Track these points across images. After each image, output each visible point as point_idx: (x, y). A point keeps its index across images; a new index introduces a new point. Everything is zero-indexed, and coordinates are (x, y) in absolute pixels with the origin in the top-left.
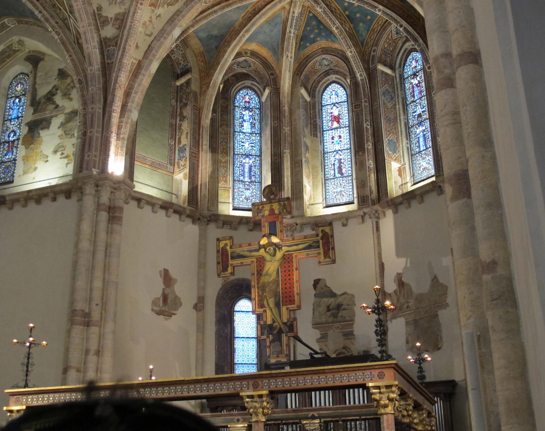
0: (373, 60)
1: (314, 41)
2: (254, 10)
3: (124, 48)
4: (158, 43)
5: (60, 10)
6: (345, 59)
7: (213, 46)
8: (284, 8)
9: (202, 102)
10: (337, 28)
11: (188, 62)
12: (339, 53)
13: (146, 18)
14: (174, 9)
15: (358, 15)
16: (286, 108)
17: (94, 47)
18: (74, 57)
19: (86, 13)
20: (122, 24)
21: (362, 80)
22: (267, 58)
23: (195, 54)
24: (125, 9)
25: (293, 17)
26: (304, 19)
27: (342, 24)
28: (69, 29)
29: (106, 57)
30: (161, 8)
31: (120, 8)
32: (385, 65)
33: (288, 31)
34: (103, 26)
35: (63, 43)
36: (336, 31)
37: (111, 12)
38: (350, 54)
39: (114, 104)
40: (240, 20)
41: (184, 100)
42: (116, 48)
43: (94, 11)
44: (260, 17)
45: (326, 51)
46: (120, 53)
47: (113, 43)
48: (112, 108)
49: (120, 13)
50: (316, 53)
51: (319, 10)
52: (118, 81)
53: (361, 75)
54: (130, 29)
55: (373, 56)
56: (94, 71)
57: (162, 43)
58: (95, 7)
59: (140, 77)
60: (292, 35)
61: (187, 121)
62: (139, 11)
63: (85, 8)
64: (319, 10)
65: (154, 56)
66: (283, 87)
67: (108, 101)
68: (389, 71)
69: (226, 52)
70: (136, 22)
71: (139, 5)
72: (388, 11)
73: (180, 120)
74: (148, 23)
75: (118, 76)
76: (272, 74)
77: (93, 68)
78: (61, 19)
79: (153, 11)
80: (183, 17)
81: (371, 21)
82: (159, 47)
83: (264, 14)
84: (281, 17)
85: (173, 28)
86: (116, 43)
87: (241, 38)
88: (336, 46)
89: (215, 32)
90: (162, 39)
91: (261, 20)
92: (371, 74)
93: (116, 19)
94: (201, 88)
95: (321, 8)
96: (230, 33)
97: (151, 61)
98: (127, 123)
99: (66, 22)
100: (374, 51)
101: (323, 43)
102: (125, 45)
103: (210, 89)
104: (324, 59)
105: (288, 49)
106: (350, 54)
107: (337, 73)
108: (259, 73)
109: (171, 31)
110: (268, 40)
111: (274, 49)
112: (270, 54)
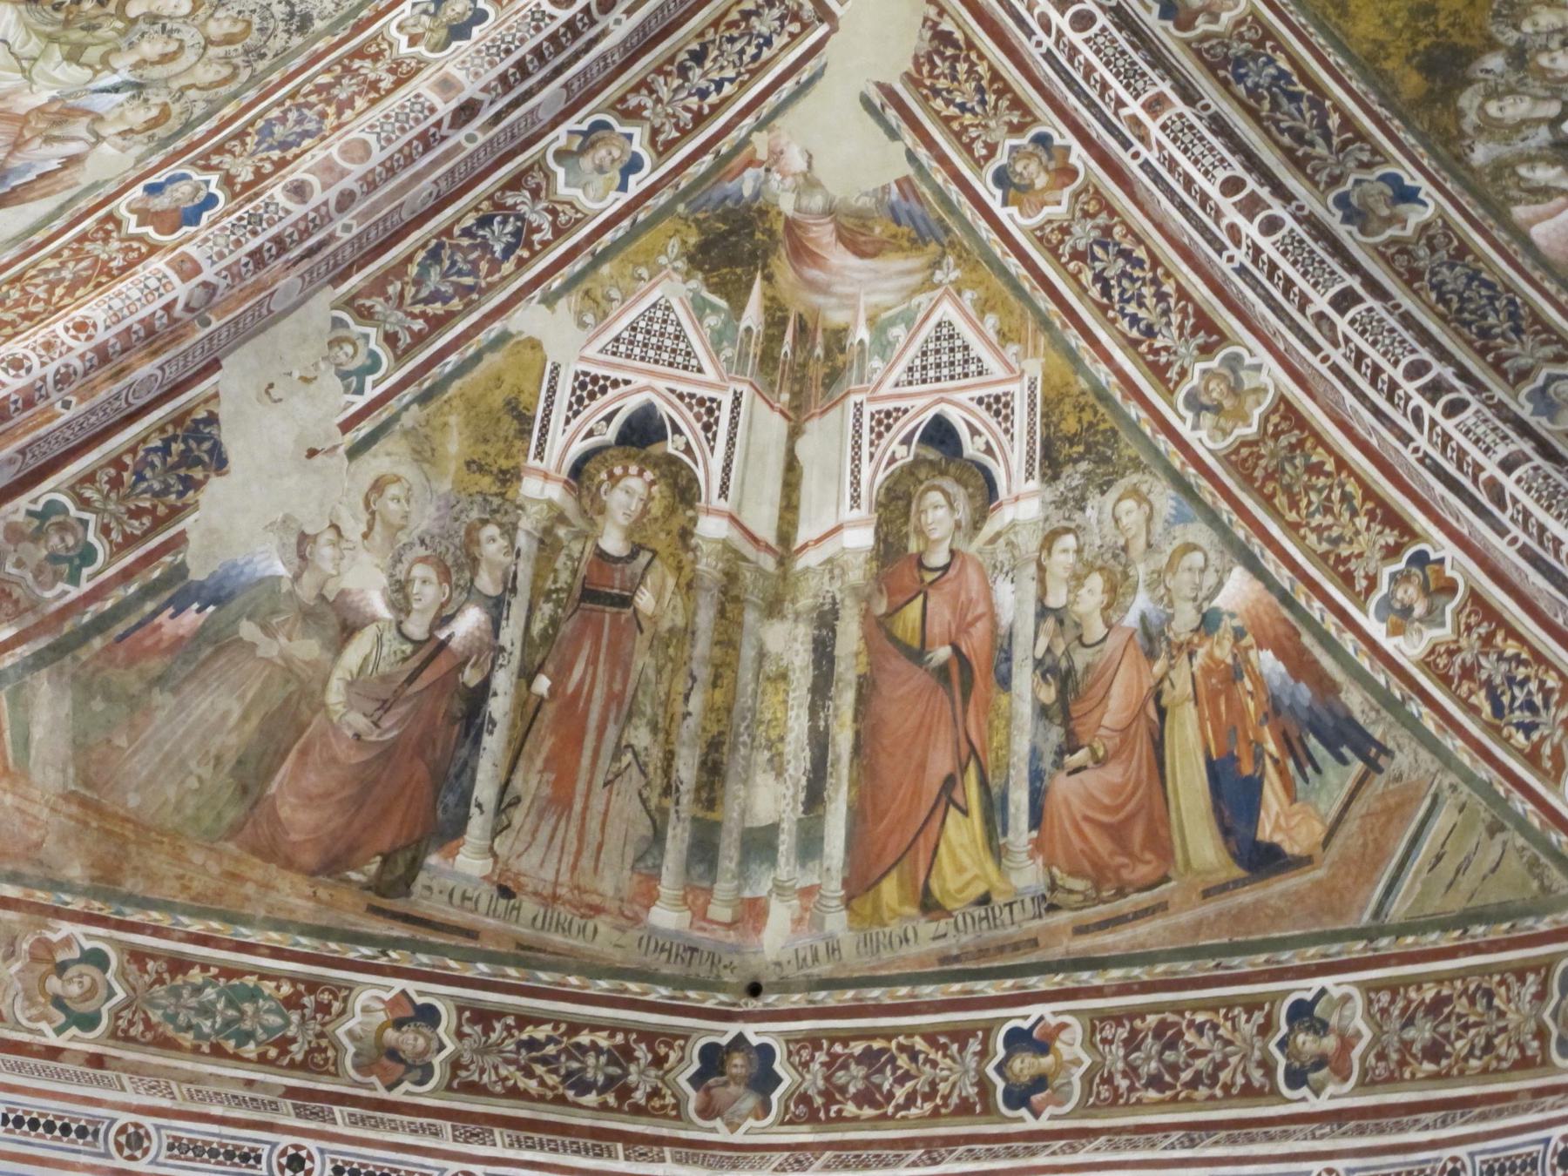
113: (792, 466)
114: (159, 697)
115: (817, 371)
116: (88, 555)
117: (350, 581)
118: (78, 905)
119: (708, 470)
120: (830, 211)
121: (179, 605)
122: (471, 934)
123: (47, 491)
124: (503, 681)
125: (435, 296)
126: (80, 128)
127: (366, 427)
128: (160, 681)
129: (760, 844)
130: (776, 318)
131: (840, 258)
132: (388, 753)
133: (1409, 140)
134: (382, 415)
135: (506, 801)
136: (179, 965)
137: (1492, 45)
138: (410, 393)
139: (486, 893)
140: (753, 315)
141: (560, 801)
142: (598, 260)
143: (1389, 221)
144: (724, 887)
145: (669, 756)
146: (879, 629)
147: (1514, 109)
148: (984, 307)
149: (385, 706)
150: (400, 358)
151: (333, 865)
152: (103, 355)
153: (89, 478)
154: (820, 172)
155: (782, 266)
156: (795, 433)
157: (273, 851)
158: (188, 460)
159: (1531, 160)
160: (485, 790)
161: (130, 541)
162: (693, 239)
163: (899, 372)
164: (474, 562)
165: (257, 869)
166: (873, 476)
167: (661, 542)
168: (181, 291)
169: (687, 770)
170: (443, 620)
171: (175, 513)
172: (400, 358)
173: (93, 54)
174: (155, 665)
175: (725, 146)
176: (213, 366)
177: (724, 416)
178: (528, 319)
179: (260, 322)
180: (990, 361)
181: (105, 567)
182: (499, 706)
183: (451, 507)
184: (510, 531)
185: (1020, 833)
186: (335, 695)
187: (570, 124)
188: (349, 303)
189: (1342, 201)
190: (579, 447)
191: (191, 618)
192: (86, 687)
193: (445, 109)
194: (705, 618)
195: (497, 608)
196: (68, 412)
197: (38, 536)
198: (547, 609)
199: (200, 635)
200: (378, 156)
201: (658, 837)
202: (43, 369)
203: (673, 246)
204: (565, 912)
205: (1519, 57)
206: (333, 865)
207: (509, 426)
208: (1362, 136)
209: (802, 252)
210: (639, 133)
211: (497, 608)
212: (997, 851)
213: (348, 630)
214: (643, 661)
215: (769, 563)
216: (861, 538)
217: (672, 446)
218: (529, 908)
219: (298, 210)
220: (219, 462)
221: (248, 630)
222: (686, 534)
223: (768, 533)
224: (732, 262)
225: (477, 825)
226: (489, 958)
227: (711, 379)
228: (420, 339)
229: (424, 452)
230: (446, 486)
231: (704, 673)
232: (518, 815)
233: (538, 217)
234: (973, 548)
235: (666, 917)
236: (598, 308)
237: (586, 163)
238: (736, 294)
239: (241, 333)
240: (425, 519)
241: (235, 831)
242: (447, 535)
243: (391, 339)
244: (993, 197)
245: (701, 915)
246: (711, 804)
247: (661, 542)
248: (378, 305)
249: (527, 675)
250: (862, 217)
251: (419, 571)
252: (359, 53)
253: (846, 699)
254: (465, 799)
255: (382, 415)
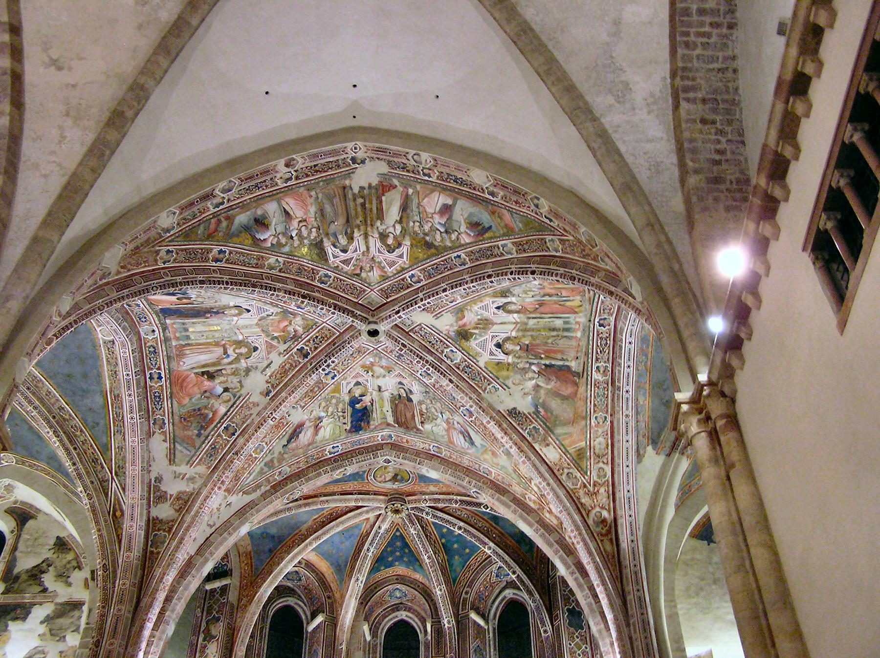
0: (464, 604)
1: (390, 565)
2: (331, 514)
3: (182, 539)
4: (220, 539)
5: (103, 467)
6: (428, 595)
7: (267, 548)
8: (368, 519)
9: (238, 620)
10: (429, 558)
11: (228, 562)
12: (419, 586)
13: (215, 506)
14: (248, 499)
15: (456, 546)
16: (344, 646)
17: (140, 528)
18: (104, 533)
19: (143, 482)
20: (185, 506)
21: (449, 628)
22: (326, 575)
23: (239, 553)
24: (194, 489)
25: (377, 533)
26: (389, 537)
27: (435, 553)
28: (106, 495)
29: (150, 543)
30: (235, 495)
31: (188, 485)
32: (478, 613)
33: (366, 547)
34: (156, 503)
35: (94, 511)
36: (427, 561)
37: (173, 488)
38: (439, 593)
39: (151, 610)
40: (310, 523)
41: (214, 613)
42: (169, 535)
43: (151, 480)
44: (337, 526)
45: (402, 580)
46: (175, 543)
47: (166, 527)
48: (147, 614)
49: (185, 492)
50: (390, 581)
51: (412, 531)
52: (164, 580)
53: (449, 622)
54: (196, 515)
55: (465, 600)
56: (131, 559)
57: (225, 539)
58: (153, 476)
59: (189, 578)
60: (370, 554)
61: (215, 644)
62: (214, 496)
63: (143, 476)
64: (412, 531)
65: (212, 554)
66: (344, 617)
67: (142, 604)
68: (481, 622)
69: (283, 559)
70: (206, 508)
71: (216, 488)
72: (500, 552)
73: (204, 640)
74: (215, 510)
75: (164, 574)
76: (329, 597)
77: (132, 554)
78: (99, 479)
79: (226, 497)
80: (258, 511)
81: (469, 555)
82: (221, 544)
83: (342, 523)
84: (361, 529)
85: (242, 523)
86: (170, 529)
87: (306, 546)
88: (418, 576)
89: (273, 531)
90: (225, 534)
91: (335, 529)
92: (461, 622)
93: (178, 498)
94: (240, 600)
95: (415, 529)
96: (294, 536)
97: (206, 560)
98: (160, 639)
99: (106, 484)
100: (467, 593)
101: (400, 569)
102: (184, 534)
103: (253, 604)
104: (397, 589)
105: (359, 571)
106: (439, 593)
107: (409, 609)
108: (310, 591)
109: (238, 527)
110: (334, 552)
111: (340, 566)
112: (332, 570)
113: (502, 323)
114: (554, 413)
115: (485, 322)
116: (534, 427)
117: (531, 387)
118: (589, 422)
119: (504, 336)
120: (457, 322)
121: (539, 412)
122: (584, 363)
123: (526, 435)
124: (543, 362)
125: (480, 378)
126: (451, 421)
127: (505, 387)
128: (552, 413)
129: (566, 323)
130: (477, 328)
131: (465, 320)
132: (557, 378)
133: (445, 254)
134: (502, 385)
135: (562, 359)
136: (595, 405)
137: (424, 238)
138: (498, 381)
139: (578, 361)
140: (476, 331)
141: (562, 352)
142: (469, 355)
143: (465, 259)
144: (573, 326)
145: (553, 336)
146: (531, 312)
147: (438, 237)
148: (475, 304)
149: (550, 379)
150: (492, 383)
151: (576, 384)
152: (506, 433)
153: (522, 429)
154: (450, 324)
155: (467, 328)
156: (496, 324)
157: (575, 393)
158: (515, 413)
159: (450, 238)
160: (561, 363)
161: (531, 421)
162: (463, 341)
163: (487, 313)
164: (524, 368)
165: (578, 396)
166: (505, 314)
167: (517, 341)
168: (492, 423)
169: (555, 333)
170: (534, 372)
171: (524, 414)
172: (492, 383)
173: (435, 417)
174: (549, 415)
175: (446, 337)
176: (499, 411)
177: (494, 334)
178: (482, 364)
179: (490, 406)
180: (486, 303)
181: (535, 424)
182: (547, 362)
183: (516, 372)
184: (518, 363)
185: (571, 298)
186: (549, 387)
187: (446, 360)
188: (484, 391)
189: (460, 265)
190: (502, 354)
191: (541, 410)
192: (555, 425)
193: (451, 385)
194: (529, 333)
195: (531, 364)
196: (515, 437)
197: (533, 435)
198: (530, 356)
199: (543, 408)
200: (462, 395)
201: (566, 337)
202: (511, 443)
203: (465, 344)
204: (580, 349)
205: (426, 234)
206: (576, 384)
207: (500, 365)
208: (446, 260)
209: (464, 325)
210: (445, 350)
211: (531, 364)
212: (573, 300)
213: (538, 386)
214: (538, 342)
215: (519, 325)
216: (515, 315)
217: (501, 341)
218: (579, 354)
219: (474, 406)
220: (515, 409)
221: (541, 401)
222: (515, 338)
223: (514, 326)
224: (467, 335)
225: (567, 363)
226: (588, 360)
227: (488, 336)
228: (488, 380)
229: (508, 378)
230: (512, 374)
231: (538, 333)
232: (564, 358)
233: (464, 364)
234: (519, 304)
235: (579, 334)
236: (478, 354)
237: (452, 358)
238: (472, 334)
239: (494, 409)
240: (518, 376)
241: (573, 399)
242: (520, 373)
243: (489, 384)
244: (454, 303)
245: (578, 330)
246: (560, 329)
247: (517, 341)
248: (483, 388)
249: (542, 358)
250: (457, 318)
251: (527, 376)
252: (434, 387)
253: (543, 315)
254: (563, 366)
255: (502, 385)
